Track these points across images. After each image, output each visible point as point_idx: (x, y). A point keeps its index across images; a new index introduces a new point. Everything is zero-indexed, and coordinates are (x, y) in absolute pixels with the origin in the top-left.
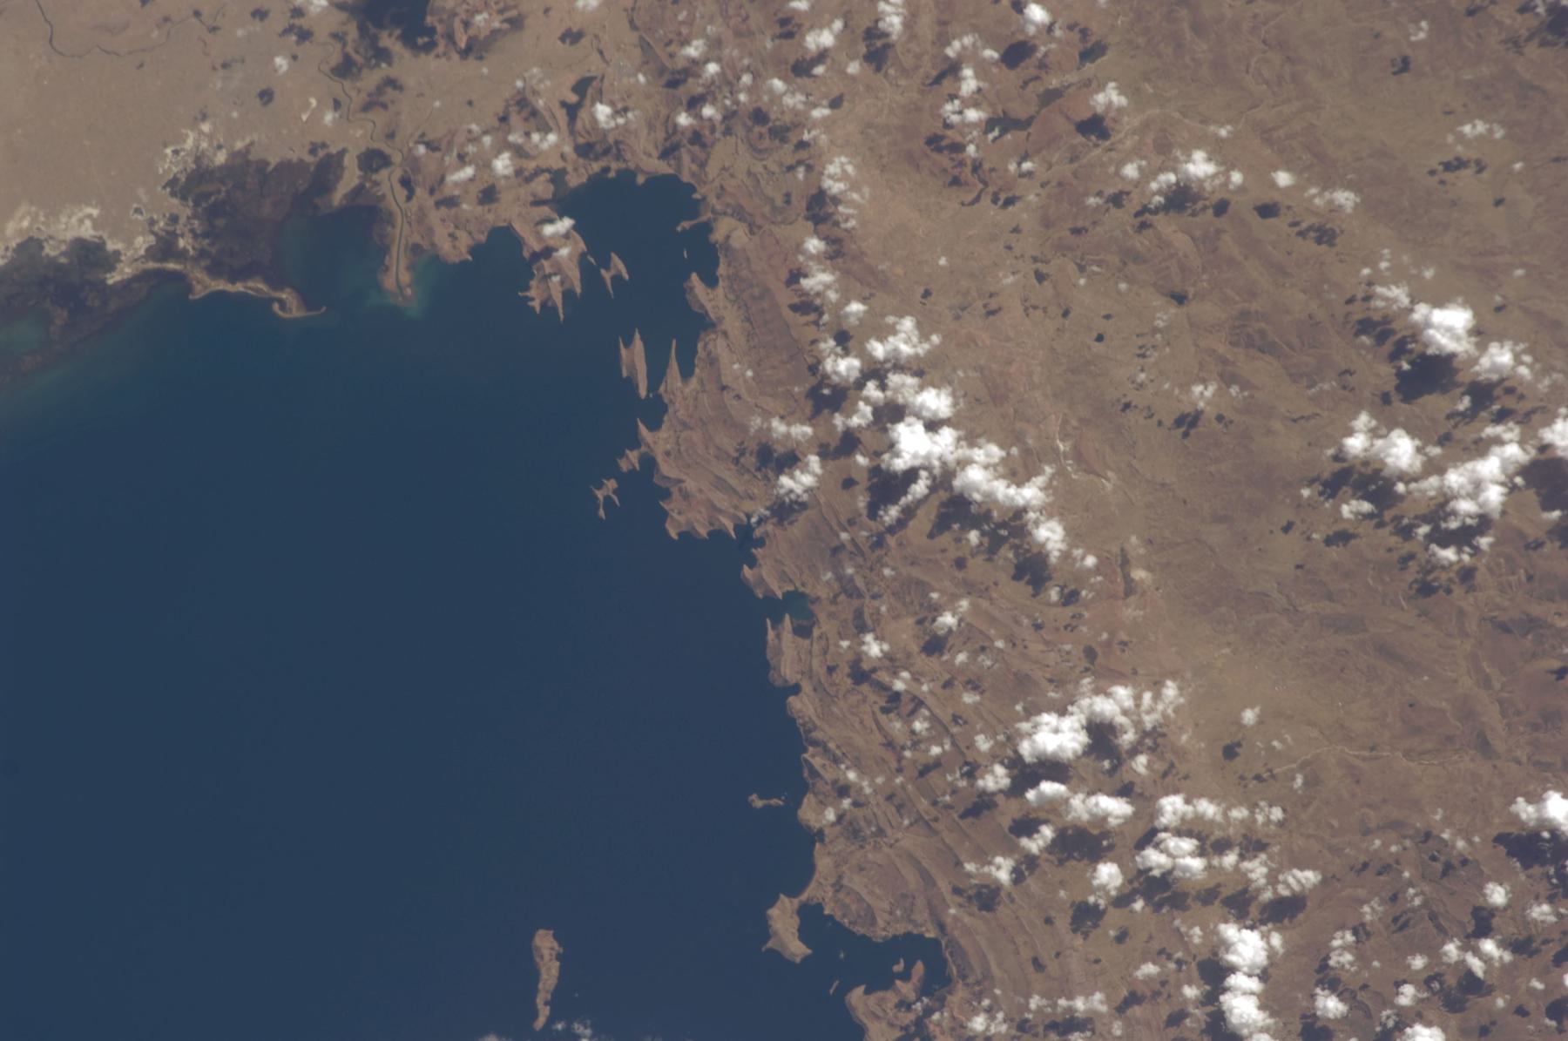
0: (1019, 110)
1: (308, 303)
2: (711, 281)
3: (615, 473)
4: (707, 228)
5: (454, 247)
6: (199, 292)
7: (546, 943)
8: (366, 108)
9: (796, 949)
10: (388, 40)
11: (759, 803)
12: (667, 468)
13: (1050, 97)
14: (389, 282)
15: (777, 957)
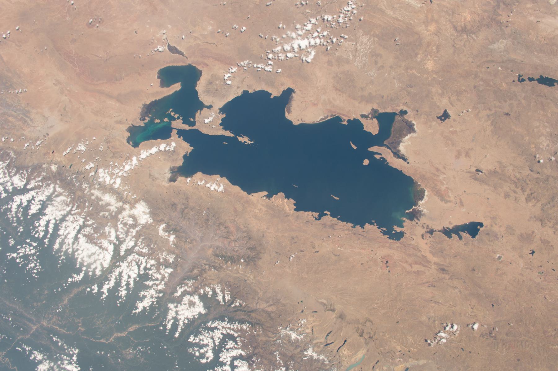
0: (387, 264)
1: (407, 213)
2: (388, 237)
3: (375, 223)
4: (393, 240)
5: (404, 224)
6: (413, 207)
7: (338, 199)
8: (423, 226)
9: (325, 212)
10: (428, 230)
11: (339, 216)
12: (372, 226)
13: (387, 267)
14: (404, 218)
15: (326, 211)
